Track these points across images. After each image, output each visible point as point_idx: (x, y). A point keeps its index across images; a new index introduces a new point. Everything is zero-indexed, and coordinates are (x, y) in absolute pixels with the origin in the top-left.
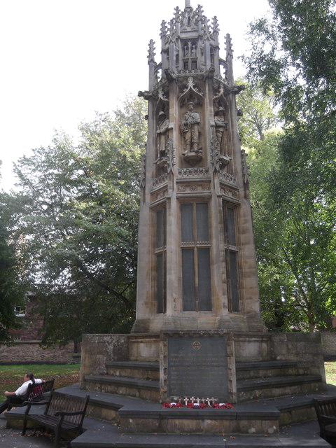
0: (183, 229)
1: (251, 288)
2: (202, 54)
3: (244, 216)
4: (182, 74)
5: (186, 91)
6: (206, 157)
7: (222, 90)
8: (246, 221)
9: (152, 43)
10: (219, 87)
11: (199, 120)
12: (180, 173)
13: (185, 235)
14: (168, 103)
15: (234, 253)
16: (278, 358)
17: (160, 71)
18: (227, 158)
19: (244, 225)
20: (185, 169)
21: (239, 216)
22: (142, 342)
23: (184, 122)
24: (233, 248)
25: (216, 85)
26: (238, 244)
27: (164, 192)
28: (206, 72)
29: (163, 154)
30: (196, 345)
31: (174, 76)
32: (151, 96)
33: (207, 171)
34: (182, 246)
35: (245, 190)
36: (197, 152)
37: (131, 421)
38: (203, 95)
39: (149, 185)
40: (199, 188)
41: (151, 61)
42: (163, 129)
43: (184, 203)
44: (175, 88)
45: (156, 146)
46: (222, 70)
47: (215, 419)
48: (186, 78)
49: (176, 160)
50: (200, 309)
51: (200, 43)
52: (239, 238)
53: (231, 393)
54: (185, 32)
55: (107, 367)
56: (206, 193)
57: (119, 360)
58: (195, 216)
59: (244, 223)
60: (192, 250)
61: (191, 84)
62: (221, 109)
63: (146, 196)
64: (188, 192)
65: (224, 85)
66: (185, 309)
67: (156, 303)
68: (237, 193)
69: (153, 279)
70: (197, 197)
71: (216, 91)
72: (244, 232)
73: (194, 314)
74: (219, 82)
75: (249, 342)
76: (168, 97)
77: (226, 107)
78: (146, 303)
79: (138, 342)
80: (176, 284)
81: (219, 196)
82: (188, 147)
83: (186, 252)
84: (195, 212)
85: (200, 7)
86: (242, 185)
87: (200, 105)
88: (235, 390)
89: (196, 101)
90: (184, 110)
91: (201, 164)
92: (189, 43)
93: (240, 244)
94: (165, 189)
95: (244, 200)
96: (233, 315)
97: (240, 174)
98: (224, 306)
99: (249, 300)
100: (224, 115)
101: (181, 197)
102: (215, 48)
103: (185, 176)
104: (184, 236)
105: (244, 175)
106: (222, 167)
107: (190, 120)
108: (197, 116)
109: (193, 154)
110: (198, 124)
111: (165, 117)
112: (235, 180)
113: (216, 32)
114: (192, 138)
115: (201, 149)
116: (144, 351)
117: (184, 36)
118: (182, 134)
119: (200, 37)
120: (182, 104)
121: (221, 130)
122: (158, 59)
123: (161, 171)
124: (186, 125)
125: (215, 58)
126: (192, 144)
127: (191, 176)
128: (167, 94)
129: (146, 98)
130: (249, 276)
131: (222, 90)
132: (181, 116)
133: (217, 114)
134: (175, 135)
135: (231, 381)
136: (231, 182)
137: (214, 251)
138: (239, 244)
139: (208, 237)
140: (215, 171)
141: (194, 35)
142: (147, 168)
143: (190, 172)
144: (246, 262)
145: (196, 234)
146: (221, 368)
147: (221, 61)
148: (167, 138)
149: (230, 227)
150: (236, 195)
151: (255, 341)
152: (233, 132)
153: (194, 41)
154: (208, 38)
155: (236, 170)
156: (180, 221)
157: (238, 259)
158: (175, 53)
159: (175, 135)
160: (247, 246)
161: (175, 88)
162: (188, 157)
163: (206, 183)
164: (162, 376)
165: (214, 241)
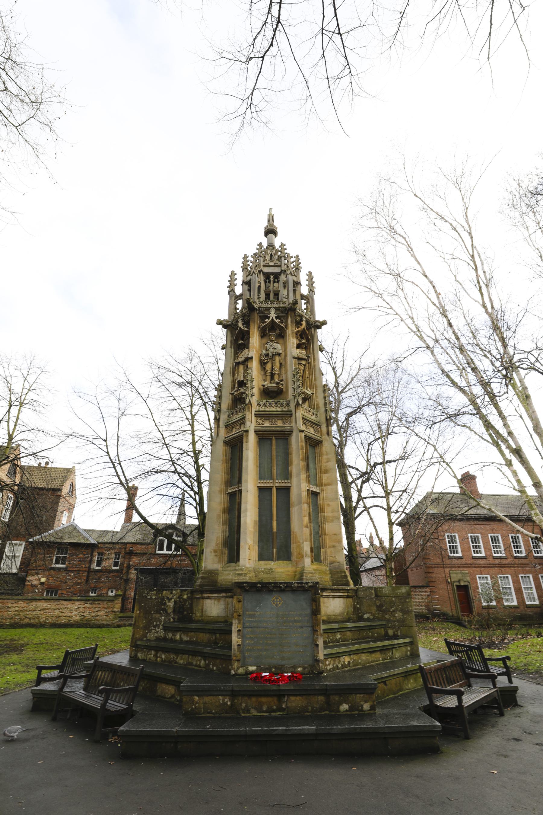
1: (335, 534)
2: (285, 287)
3: (327, 454)
4: (264, 305)
7: (304, 324)
9: (233, 274)
10: (302, 320)
11: (280, 352)
12: (259, 404)
13: (263, 473)
14: (248, 333)
15: (315, 494)
16: (366, 616)
17: (240, 302)
18: (309, 392)
20: (264, 401)
21: (321, 455)
22: (209, 598)
23: (264, 352)
24: (314, 489)
25: (299, 318)
26: (320, 484)
27: (241, 424)
28: (289, 305)
29: (242, 384)
31: (256, 306)
32: (229, 325)
33: (288, 404)
34: (259, 485)
35: (327, 426)
36: (278, 383)
37: (196, 698)
38: (286, 326)
39: (224, 417)
41: (231, 291)
42: (241, 359)
43: (263, 437)
44: (256, 318)
45: (233, 375)
46: (303, 305)
48: (268, 309)
50: (278, 559)
51: (283, 278)
52: (321, 479)
53: (318, 661)
54: (267, 266)
56: (287, 426)
58: (274, 452)
59: (327, 462)
60: (270, 489)
61: (273, 315)
62: (304, 341)
63: (220, 429)
65: (306, 318)
66: (261, 557)
68: (320, 429)
69: (224, 524)
70: (277, 431)
71: (298, 323)
72: (326, 472)
73: (272, 564)
74: (301, 316)
75: (334, 597)
76: (248, 326)
77: (308, 340)
78: (215, 551)
79: (203, 598)
82: (269, 378)
83: (263, 491)
84: (274, 447)
85: (282, 245)
86: (323, 420)
87: (282, 336)
89: (278, 331)
90: (264, 340)
91: (282, 397)
92: (272, 277)
93: (322, 485)
94: (242, 421)
95: (326, 436)
96: (314, 567)
97: (322, 409)
98: (306, 555)
99: (332, 549)
100: (306, 348)
101: (260, 431)
102: (297, 284)
104: (261, 477)
105: (326, 411)
106: (304, 400)
107: (271, 350)
108: (278, 347)
109: (274, 385)
110: (279, 354)
111: (246, 346)
112: (316, 415)
113: (298, 268)
114: (272, 369)
115: (282, 381)
117: (266, 270)
118: (263, 364)
119: (283, 272)
120: (263, 334)
121: (303, 362)
122: (239, 290)
123: (238, 402)
124: (267, 355)
125: (297, 293)
126: (272, 375)
128: (247, 323)
129: (225, 326)
131: (304, 324)
132: (263, 346)
133: (298, 346)
134: (255, 365)
135: (317, 646)
136: (314, 418)
138: (322, 485)
139: (287, 475)
140: (297, 405)
141: (277, 269)
142: (223, 399)
144: (328, 505)
145: (275, 471)
146: (305, 629)
147: (303, 297)
148: (246, 368)
149: (311, 465)
150: (318, 431)
151: (339, 597)
152: (314, 366)
153: (277, 276)
154: (291, 273)
155: (317, 405)
156: (258, 456)
157: (320, 502)
158: (257, 285)
159: (255, 365)
160: (329, 487)
161: (256, 318)
162: (268, 388)
163: (287, 416)
164: (235, 639)
165: (294, 480)
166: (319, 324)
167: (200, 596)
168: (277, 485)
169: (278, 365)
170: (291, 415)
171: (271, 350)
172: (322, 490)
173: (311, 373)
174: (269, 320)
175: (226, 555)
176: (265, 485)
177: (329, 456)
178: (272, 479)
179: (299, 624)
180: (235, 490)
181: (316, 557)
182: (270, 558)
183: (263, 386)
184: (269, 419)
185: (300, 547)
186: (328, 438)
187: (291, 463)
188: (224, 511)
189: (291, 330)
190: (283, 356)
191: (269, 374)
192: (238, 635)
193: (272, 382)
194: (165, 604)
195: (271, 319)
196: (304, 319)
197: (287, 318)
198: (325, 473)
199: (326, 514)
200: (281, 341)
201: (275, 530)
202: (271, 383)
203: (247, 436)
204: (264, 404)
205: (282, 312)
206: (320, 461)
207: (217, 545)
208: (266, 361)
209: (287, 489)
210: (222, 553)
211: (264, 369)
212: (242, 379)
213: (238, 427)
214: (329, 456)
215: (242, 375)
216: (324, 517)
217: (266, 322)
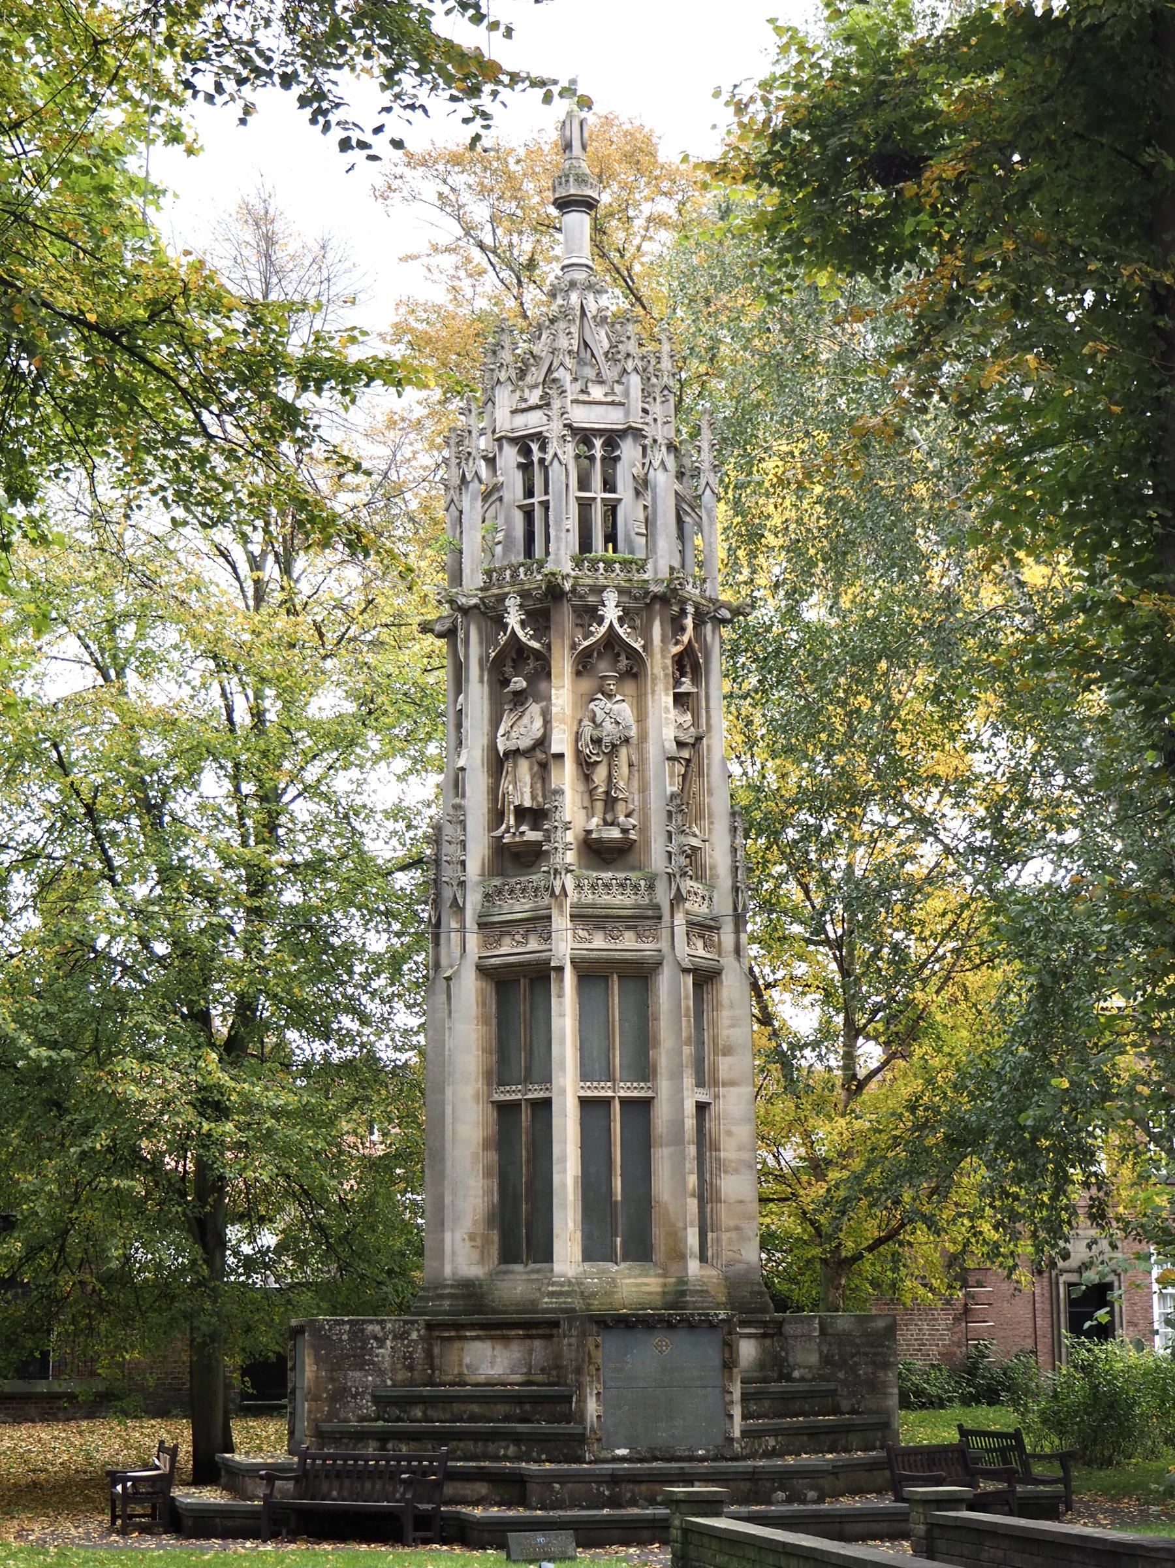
0: (583, 1048)
1: (741, 1202)
5: (601, 631)
6: (647, 843)
7: (689, 622)
10: (683, 612)
19: (731, 1031)
22: (477, 1338)
23: (588, 731)
33: (651, 887)
34: (582, 1093)
36: (625, 831)
37: (557, 1486)
49: (570, 857)
52: (715, 1069)
53: (731, 1440)
56: (648, 947)
59: (732, 1026)
60: (606, 1102)
61: (611, 613)
62: (687, 686)
66: (588, 1255)
67: (495, 1236)
68: (716, 939)
69: (488, 1174)
72: (728, 1051)
78: (472, 1237)
80: (571, 1197)
81: (686, 971)
82: (599, 806)
88: (737, 1434)
90: (586, 685)
91: (632, 858)
92: (598, 443)
93: (716, 1083)
99: (733, 1234)
101: (583, 960)
109: (616, 833)
116: (490, 1362)
117: (583, 417)
118: (585, 766)
120: (584, 664)
126: (610, 802)
130: (737, 1171)
131: (689, 622)
135: (731, 1417)
137: (662, 1114)
138: (716, 1083)
139: (644, 1070)
141: (613, 418)
143: (607, 886)
144: (729, 1133)
153: (612, 438)
159: (566, 777)
160: (733, 1090)
161: (565, 617)
162: (599, 841)
165: (664, 1086)
167: (453, 1334)
168: (622, 1094)
169: (625, 769)
171: (608, 726)
172: (717, 1097)
173: (700, 774)
174: (603, 630)
175: (496, 1246)
176: (596, 1094)
178: (610, 1078)
179: (698, 1383)
180: (514, 1097)
181: (703, 1258)
183: (589, 832)
187: (657, 1044)
188: (486, 1145)
189: (659, 664)
190: (634, 741)
191: (603, 797)
192: (598, 1400)
195: (606, 624)
196: (690, 609)
198: (724, 1055)
199: (722, 1154)
200: (630, 687)
202: (606, 823)
203: (562, 980)
205: (636, 598)
206: (714, 1024)
207: (475, 1222)
208: (594, 758)
209: (645, 1104)
210: (486, 1240)
211: (587, 778)
212: (527, 803)
213: (518, 938)
215: (527, 790)
216: (718, 1160)
217: (592, 634)
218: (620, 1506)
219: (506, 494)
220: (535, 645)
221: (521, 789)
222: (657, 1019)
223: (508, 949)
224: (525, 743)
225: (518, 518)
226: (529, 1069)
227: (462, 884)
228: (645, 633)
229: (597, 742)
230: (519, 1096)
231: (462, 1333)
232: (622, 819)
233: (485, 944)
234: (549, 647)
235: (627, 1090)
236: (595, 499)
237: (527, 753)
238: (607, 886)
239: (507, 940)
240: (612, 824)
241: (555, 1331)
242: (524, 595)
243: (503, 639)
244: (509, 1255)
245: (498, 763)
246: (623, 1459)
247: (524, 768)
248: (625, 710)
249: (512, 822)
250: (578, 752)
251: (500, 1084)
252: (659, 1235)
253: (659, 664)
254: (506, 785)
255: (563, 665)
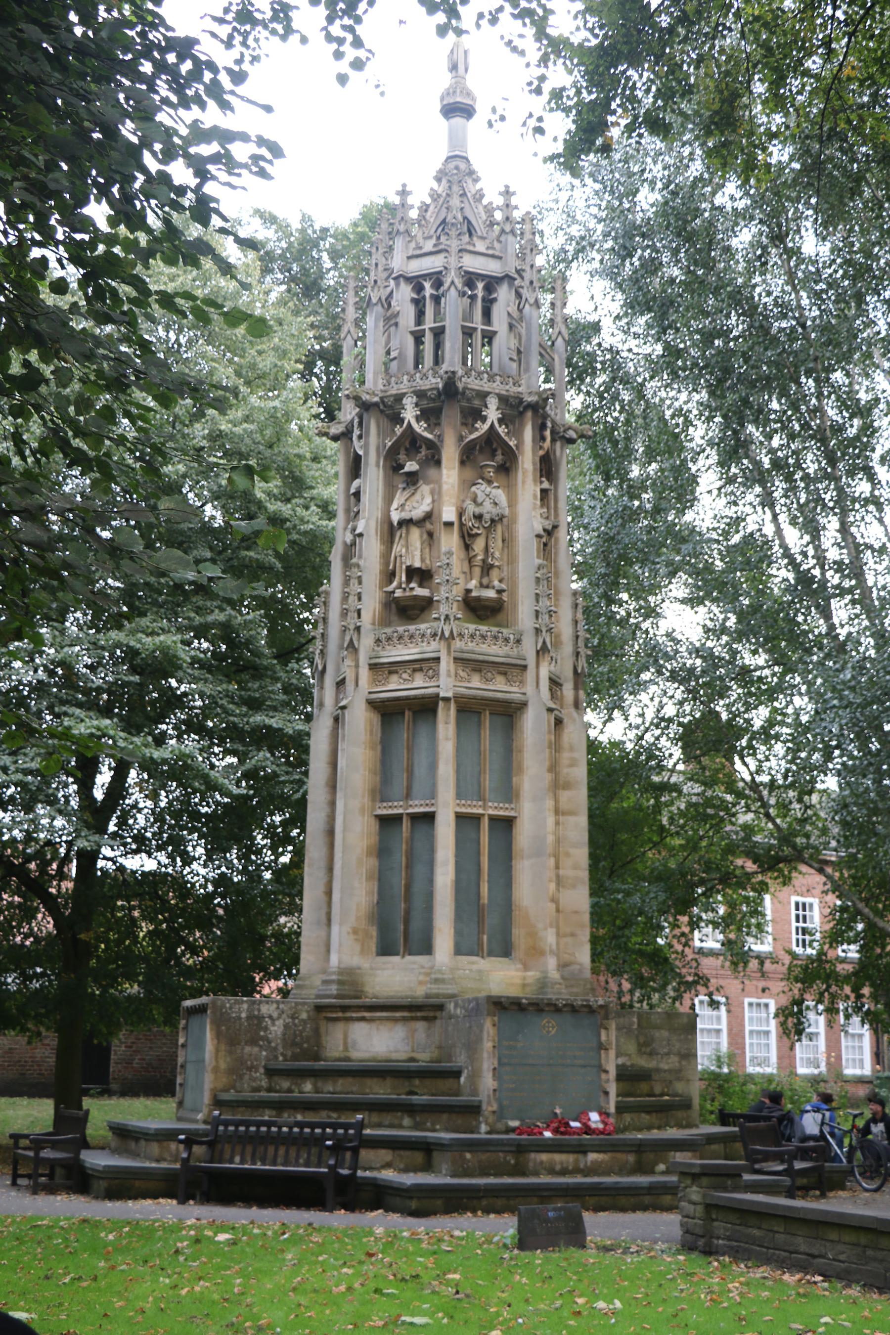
3: (572, 749)
5: (483, 428)
7: (548, 433)
8: (573, 764)
20: (472, 627)
22: (363, 1019)
23: (471, 509)
30: (549, 1025)
31: (460, 386)
33: (518, 641)
34: (458, 810)
36: (500, 592)
37: (468, 1156)
39: (366, 643)
40: (500, 679)
47: (604, 1152)
48: (483, 396)
50: (491, 954)
55: (271, 1072)
57: (295, 1058)
59: (571, 766)
60: (477, 818)
61: (493, 413)
64: (476, 685)
66: (459, 950)
67: (374, 931)
69: (369, 878)
70: (497, 700)
78: (355, 931)
82: (477, 571)
86: (569, 673)
87: (507, 467)
90: (469, 473)
91: (501, 617)
95: (572, 710)
99: (569, 940)
101: (463, 696)
103: (471, 646)
109: (491, 594)
118: (467, 538)
126: (487, 569)
127: (484, 648)
130: (574, 886)
131: (548, 433)
135: (606, 1093)
139: (509, 793)
141: (492, 268)
143: (483, 637)
144: (568, 855)
153: (492, 283)
162: (478, 599)
166: (574, 436)
167: (340, 1014)
168: (491, 812)
170: (524, 668)
174: (486, 427)
177: (575, 755)
178: (481, 797)
180: (395, 811)
182: (476, 951)
183: (468, 591)
184: (480, 671)
185: (533, 934)
186: (575, 714)
187: (520, 770)
188: (369, 854)
189: (527, 461)
193: (485, 581)
194: (266, 1029)
196: (549, 424)
197: (522, 426)
201: (485, 900)
202: (482, 585)
204: (472, 636)
208: (475, 531)
212: (417, 564)
214: (575, 755)
215: (418, 553)
218: (523, 1174)
219: (401, 320)
220: (427, 435)
221: (412, 551)
222: (520, 751)
223: (397, 687)
224: (418, 513)
225: (410, 341)
226: (409, 788)
227: (358, 629)
228: (518, 434)
229: (479, 517)
230: (401, 811)
231: (348, 1014)
232: (496, 583)
233: (374, 681)
234: (440, 437)
235: (494, 809)
236: (475, 329)
237: (419, 523)
238: (483, 637)
239: (394, 678)
240: (487, 587)
241: (438, 1014)
242: (420, 395)
243: (399, 430)
244: (386, 949)
245: (391, 531)
246: (513, 1130)
247: (416, 535)
248: (500, 495)
249: (404, 579)
250: (461, 525)
251: (382, 801)
252: (518, 934)
253: (527, 461)
254: (398, 548)
255: (450, 453)
